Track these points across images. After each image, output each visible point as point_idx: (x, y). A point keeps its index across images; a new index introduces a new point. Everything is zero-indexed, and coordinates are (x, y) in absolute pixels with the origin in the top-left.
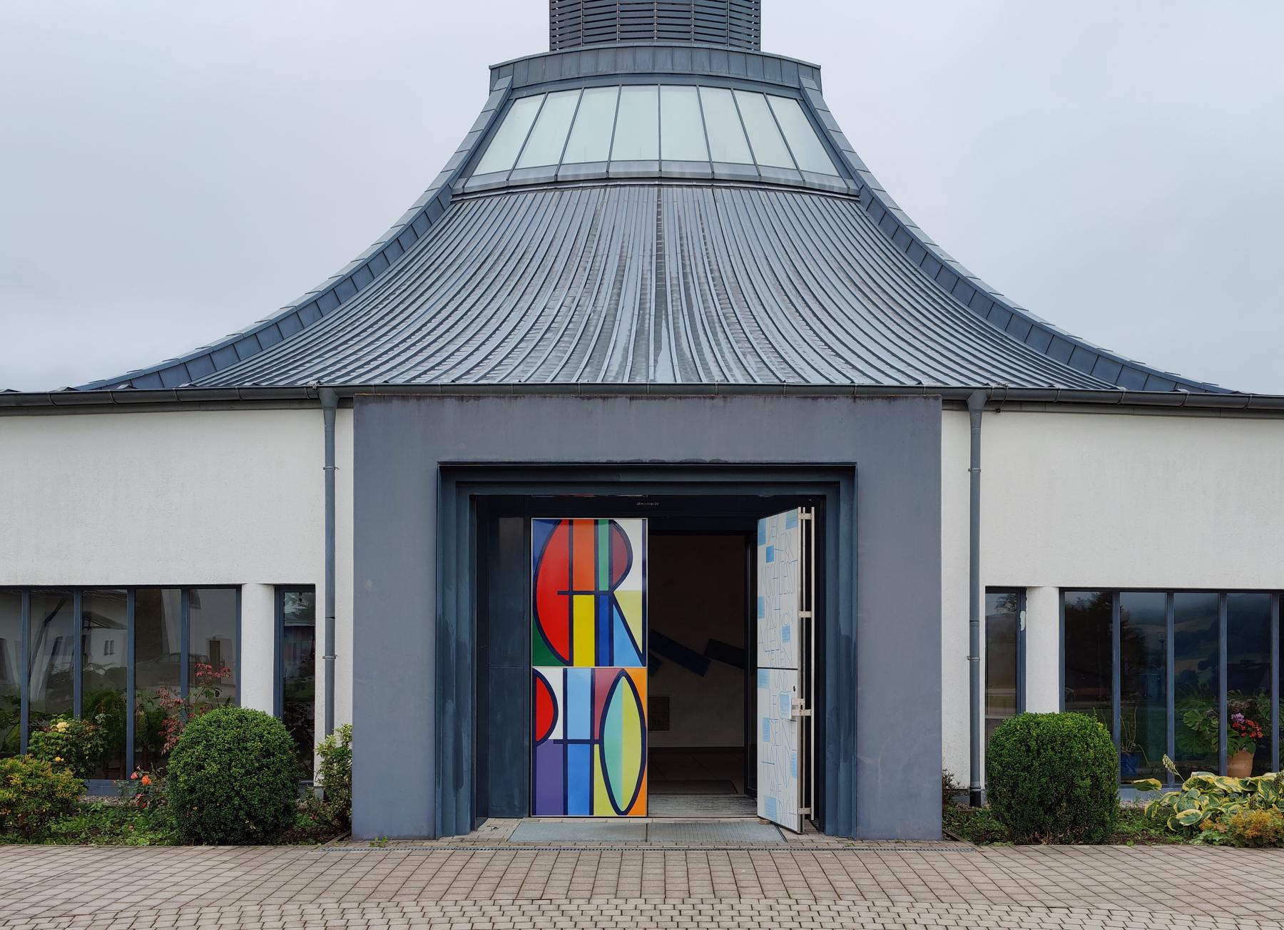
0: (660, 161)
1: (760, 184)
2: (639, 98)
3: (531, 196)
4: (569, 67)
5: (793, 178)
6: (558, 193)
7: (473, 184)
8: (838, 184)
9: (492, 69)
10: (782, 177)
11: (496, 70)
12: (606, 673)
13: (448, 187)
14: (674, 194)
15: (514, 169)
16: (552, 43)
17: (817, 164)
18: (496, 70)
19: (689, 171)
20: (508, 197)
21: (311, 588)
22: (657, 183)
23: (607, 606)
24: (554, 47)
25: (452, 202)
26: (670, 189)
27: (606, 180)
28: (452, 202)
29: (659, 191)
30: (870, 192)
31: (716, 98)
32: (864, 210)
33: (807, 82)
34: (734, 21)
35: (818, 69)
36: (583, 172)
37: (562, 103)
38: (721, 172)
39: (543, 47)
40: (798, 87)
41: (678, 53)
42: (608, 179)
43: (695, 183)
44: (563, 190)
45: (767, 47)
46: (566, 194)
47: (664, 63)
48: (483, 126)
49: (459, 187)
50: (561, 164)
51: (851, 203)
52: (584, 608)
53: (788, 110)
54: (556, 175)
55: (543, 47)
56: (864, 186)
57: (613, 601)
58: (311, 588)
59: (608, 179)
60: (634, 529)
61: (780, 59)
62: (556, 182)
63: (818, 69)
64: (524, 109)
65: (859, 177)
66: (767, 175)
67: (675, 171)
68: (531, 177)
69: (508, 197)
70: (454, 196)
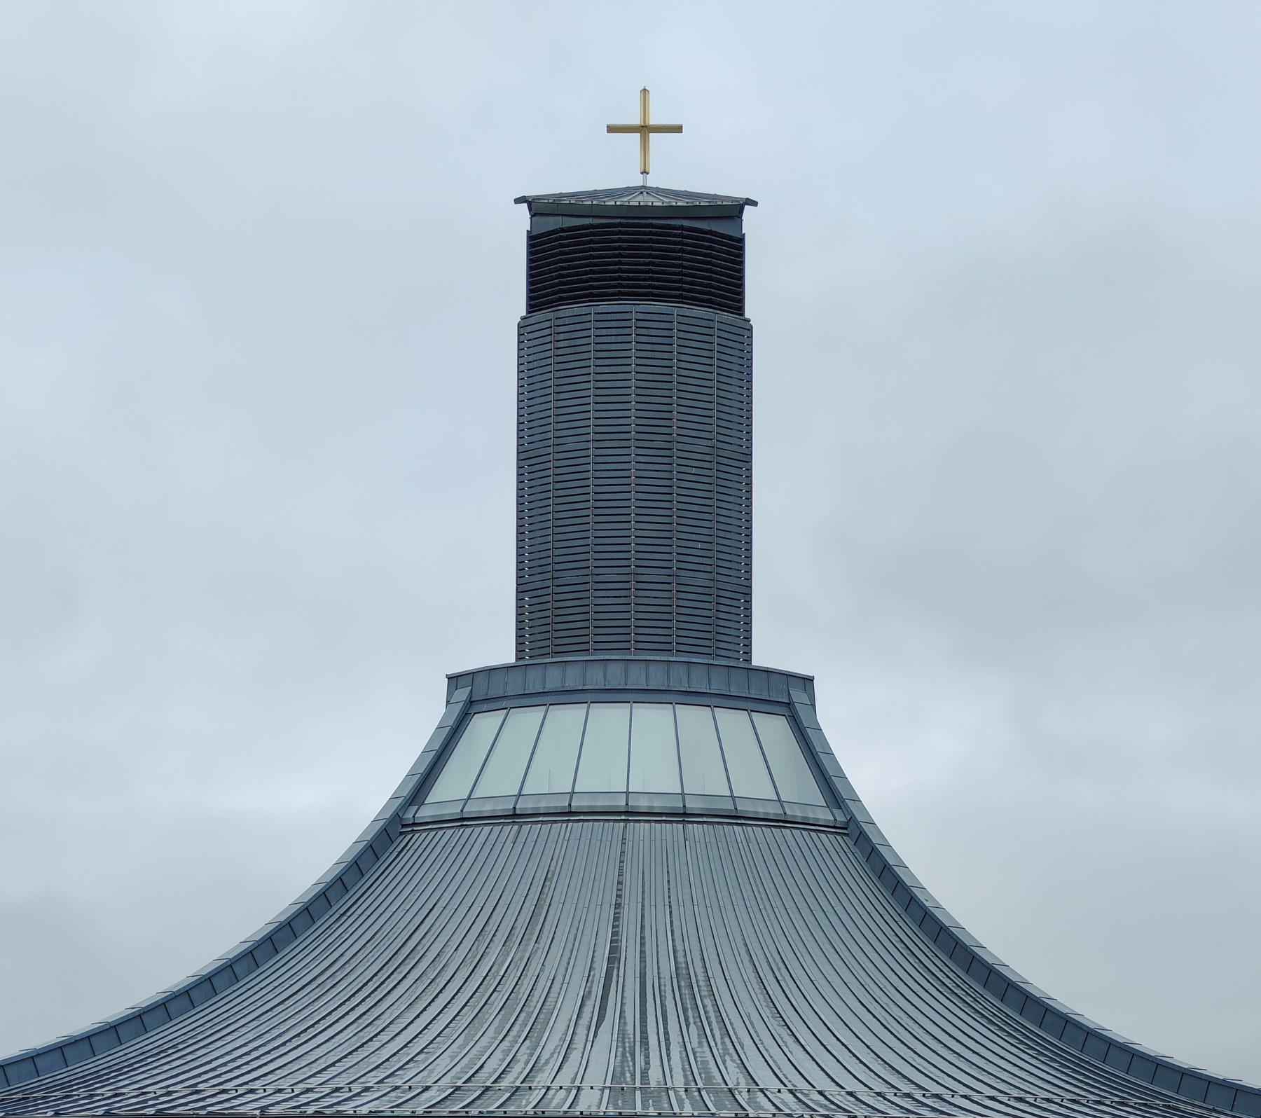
0: (628, 793)
1: (735, 817)
2: (610, 717)
3: (487, 829)
4: (534, 681)
5: (773, 810)
6: (516, 827)
7: (425, 813)
8: (824, 815)
9: (450, 678)
10: (761, 810)
11: (455, 681)
14: (642, 829)
15: (469, 798)
16: (519, 651)
18: (455, 681)
19: (658, 804)
20: (462, 830)
22: (623, 817)
24: (521, 655)
25: (401, 833)
26: (637, 825)
27: (569, 814)
28: (401, 833)
29: (625, 827)
30: (857, 824)
31: (695, 718)
32: (851, 843)
33: (798, 696)
34: (722, 623)
35: (810, 680)
36: (543, 805)
37: (526, 720)
38: (693, 805)
39: (507, 655)
40: (787, 701)
41: (652, 667)
42: (571, 813)
43: (664, 818)
44: (521, 825)
46: (526, 828)
47: (637, 678)
48: (437, 746)
49: (409, 816)
50: (520, 794)
51: (844, 837)
53: (775, 728)
54: (514, 808)
55: (507, 655)
56: (852, 818)
59: (571, 813)
61: (767, 672)
62: (515, 815)
63: (810, 680)
64: (483, 726)
65: (847, 807)
66: (743, 807)
67: (643, 804)
68: (488, 808)
69: (462, 830)
70: (404, 826)
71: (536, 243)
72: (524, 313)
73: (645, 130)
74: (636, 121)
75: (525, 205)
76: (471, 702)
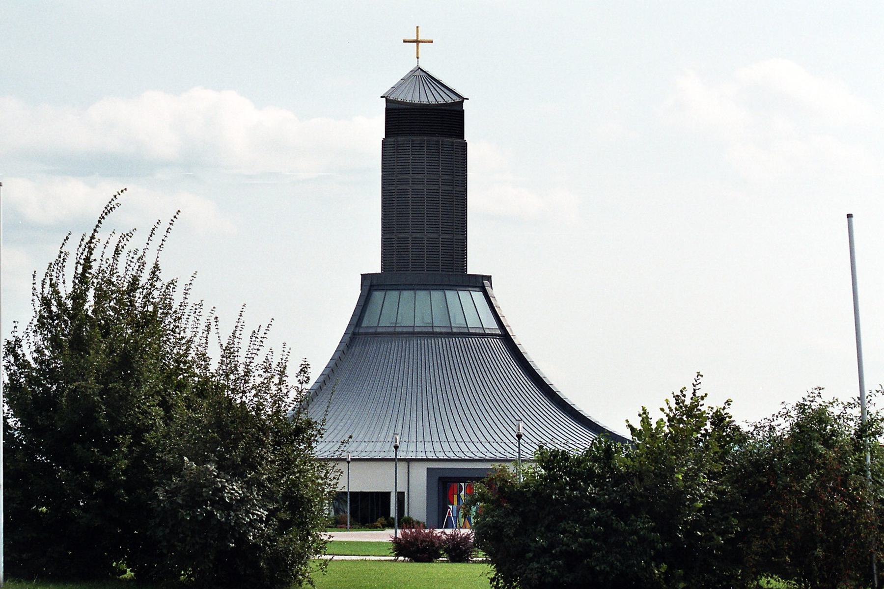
7: (362, 330)
8: (499, 332)
10: (478, 331)
12: (459, 507)
13: (354, 334)
17: (490, 324)
21: (404, 493)
23: (459, 496)
33: (486, 282)
35: (489, 278)
45: (470, 271)
52: (455, 496)
53: (478, 296)
57: (460, 495)
58: (404, 493)
60: (463, 484)
63: (489, 278)
64: (378, 295)
71: (387, 111)
72: (384, 137)
73: (417, 42)
74: (415, 38)
75: (384, 99)
76: (371, 286)
